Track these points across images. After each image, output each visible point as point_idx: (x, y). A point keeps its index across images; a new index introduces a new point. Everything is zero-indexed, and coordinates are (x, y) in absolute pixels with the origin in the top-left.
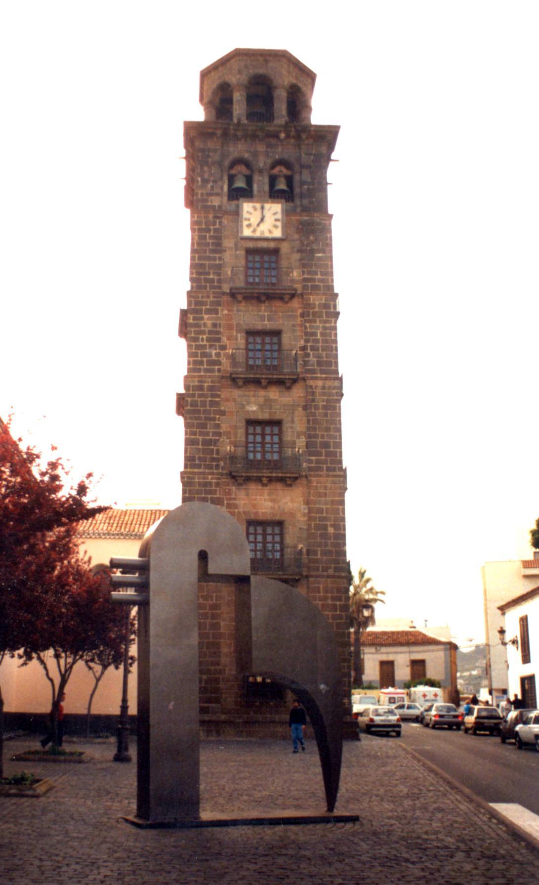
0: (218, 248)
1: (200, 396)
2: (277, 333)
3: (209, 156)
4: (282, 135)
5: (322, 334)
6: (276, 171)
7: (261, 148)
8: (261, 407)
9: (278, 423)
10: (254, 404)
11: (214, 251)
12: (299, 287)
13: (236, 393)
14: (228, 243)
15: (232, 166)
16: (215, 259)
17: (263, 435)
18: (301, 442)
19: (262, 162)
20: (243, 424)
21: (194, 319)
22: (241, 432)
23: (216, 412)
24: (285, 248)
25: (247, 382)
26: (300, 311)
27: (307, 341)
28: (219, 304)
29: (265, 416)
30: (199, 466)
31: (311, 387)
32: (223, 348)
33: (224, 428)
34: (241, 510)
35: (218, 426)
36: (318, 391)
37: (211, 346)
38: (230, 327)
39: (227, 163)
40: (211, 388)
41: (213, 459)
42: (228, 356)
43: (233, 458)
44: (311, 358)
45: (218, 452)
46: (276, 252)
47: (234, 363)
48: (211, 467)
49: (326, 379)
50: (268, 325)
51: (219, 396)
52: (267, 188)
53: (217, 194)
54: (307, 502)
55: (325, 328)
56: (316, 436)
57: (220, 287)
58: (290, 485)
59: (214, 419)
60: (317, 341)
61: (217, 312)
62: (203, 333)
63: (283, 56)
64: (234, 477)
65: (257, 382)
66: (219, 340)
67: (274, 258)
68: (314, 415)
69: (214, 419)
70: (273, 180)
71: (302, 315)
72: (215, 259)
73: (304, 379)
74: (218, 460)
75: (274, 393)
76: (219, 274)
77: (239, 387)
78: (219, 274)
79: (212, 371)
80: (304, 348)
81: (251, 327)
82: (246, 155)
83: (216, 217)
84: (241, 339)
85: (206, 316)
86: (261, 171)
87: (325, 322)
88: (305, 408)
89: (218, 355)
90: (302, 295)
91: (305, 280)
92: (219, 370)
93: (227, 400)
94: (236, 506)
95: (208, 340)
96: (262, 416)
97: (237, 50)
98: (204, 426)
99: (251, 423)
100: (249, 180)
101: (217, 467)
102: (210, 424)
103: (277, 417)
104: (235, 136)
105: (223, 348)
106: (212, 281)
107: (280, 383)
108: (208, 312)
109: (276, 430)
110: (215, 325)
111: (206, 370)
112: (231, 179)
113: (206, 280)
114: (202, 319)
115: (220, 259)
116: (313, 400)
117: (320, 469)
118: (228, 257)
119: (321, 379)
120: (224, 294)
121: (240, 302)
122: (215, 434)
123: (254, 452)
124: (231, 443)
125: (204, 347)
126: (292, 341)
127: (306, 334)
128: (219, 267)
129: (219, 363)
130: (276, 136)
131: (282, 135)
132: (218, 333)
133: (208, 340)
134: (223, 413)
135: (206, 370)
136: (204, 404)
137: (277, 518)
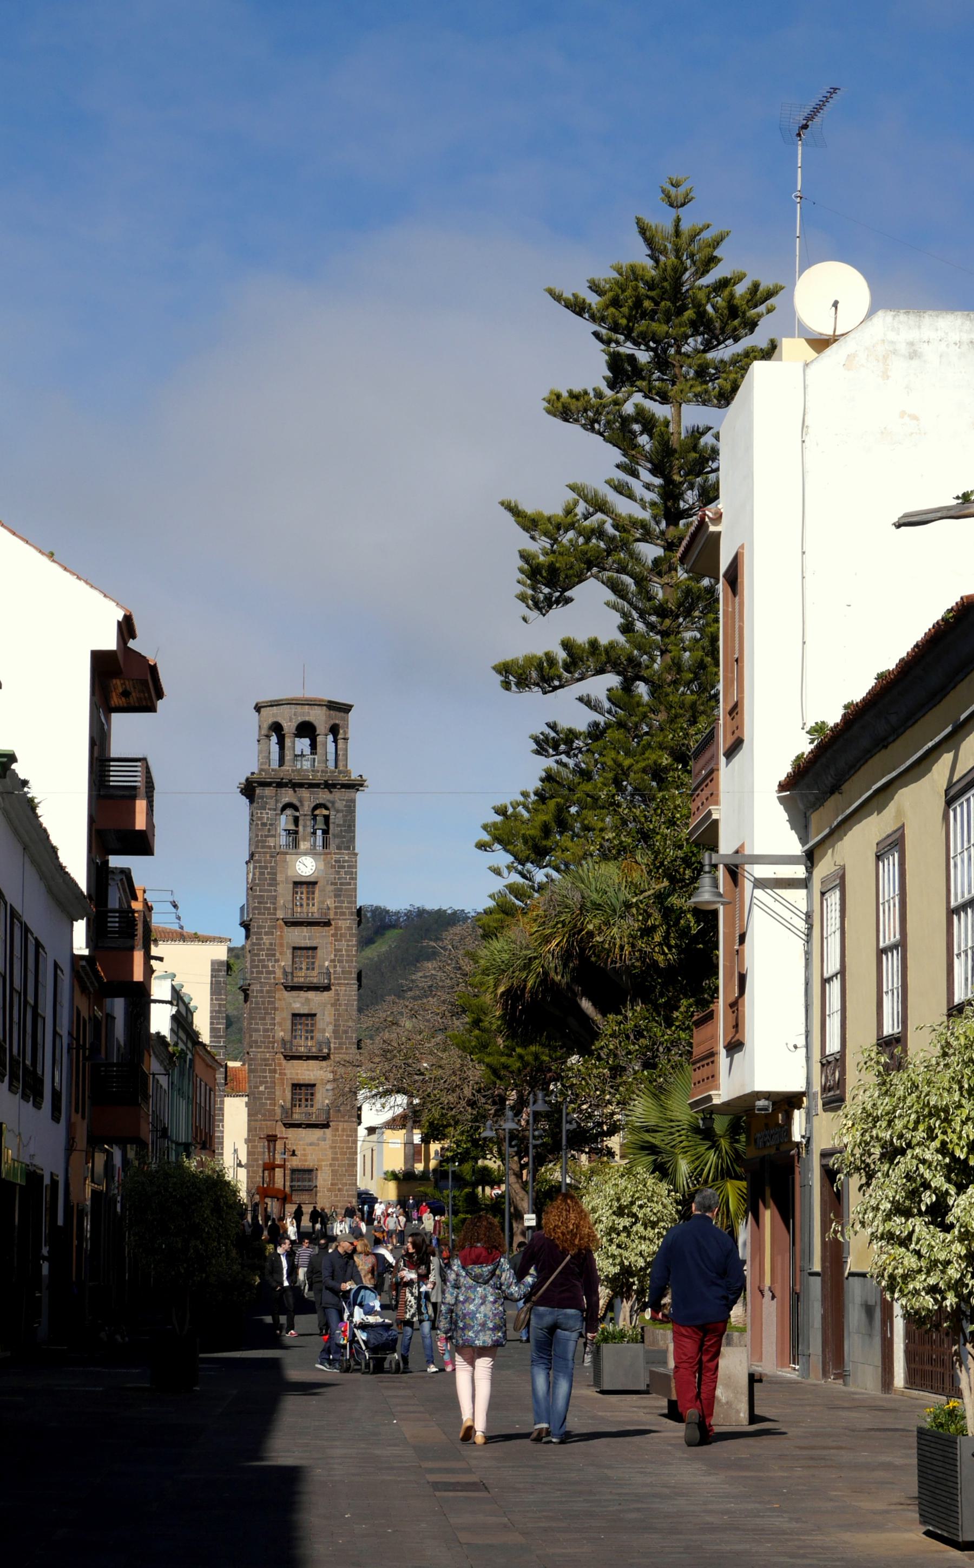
0: (274, 882)
1: (261, 997)
2: (315, 948)
3: (266, 803)
5: (346, 950)
6: (317, 812)
8: (303, 1004)
10: (298, 1002)
11: (270, 885)
13: (286, 994)
14: (280, 878)
16: (270, 891)
18: (331, 1028)
19: (306, 808)
20: (290, 1017)
21: (257, 939)
22: (289, 1023)
27: (335, 956)
28: (275, 927)
29: (306, 1012)
30: (260, 1047)
33: (277, 1020)
34: (289, 1076)
35: (274, 1019)
36: (342, 993)
37: (268, 960)
38: (281, 945)
39: (280, 805)
40: (268, 992)
41: (270, 1042)
44: (338, 969)
45: (274, 1037)
46: (315, 883)
48: (269, 1048)
50: (308, 943)
55: (348, 946)
56: (339, 1025)
57: (275, 914)
59: (271, 1014)
60: (342, 956)
61: (272, 934)
62: (263, 950)
66: (274, 955)
68: (338, 1010)
69: (271, 1014)
72: (270, 891)
75: (311, 995)
76: (274, 904)
78: (274, 904)
79: (269, 979)
80: (332, 961)
81: (297, 945)
87: (349, 941)
88: (332, 1005)
89: (273, 966)
93: (280, 1000)
94: (285, 1074)
95: (267, 955)
98: (264, 1019)
99: (295, 1015)
101: (273, 1048)
102: (268, 1017)
103: (313, 1012)
105: (277, 961)
106: (269, 909)
108: (266, 934)
110: (271, 944)
111: (265, 978)
113: (265, 908)
114: (262, 939)
115: (275, 891)
117: (342, 1048)
118: (280, 888)
127: (335, 950)
128: (275, 897)
129: (274, 972)
132: (275, 950)
133: (267, 955)
135: (265, 978)
136: (263, 1003)
137: (312, 1082)
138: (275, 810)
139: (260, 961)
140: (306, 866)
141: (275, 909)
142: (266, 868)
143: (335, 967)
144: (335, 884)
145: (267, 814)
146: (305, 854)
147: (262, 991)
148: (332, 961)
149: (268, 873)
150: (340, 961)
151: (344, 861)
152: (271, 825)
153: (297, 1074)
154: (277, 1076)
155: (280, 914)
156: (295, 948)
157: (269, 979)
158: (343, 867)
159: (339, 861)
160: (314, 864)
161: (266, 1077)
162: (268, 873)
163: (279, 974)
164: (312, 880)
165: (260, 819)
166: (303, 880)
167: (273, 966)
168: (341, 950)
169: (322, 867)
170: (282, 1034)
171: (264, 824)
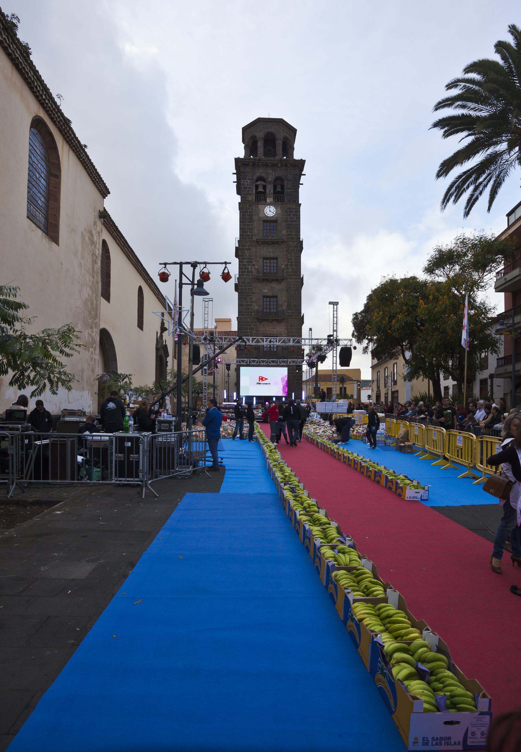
0: (251, 220)
2: (276, 259)
4: (279, 165)
7: (270, 171)
9: (276, 297)
11: (249, 222)
12: (285, 238)
14: (255, 218)
15: (257, 181)
17: (270, 301)
19: (270, 178)
23: (251, 293)
24: (280, 221)
25: (263, 280)
26: (286, 249)
27: (288, 262)
29: (271, 294)
30: (244, 315)
31: (289, 282)
32: (254, 265)
35: (251, 299)
37: (248, 265)
42: (255, 268)
43: (257, 312)
44: (290, 270)
45: (252, 309)
47: (258, 272)
49: (296, 278)
50: (272, 255)
51: (252, 286)
52: (272, 191)
53: (251, 194)
54: (287, 329)
57: (252, 238)
58: (280, 322)
59: (250, 296)
60: (292, 262)
62: (245, 259)
63: (281, 122)
64: (258, 319)
65: (267, 280)
66: (252, 262)
67: (275, 224)
69: (250, 296)
70: (275, 187)
71: (286, 251)
73: (287, 279)
74: (251, 312)
75: (274, 285)
76: (252, 233)
77: (260, 282)
78: (252, 233)
80: (287, 265)
82: (263, 175)
83: (250, 206)
84: (261, 261)
85: (246, 252)
86: (270, 183)
88: (287, 291)
89: (251, 268)
90: (286, 242)
91: (288, 235)
92: (252, 275)
94: (259, 331)
96: (269, 294)
97: (259, 118)
99: (264, 297)
100: (265, 187)
103: (275, 295)
104: (259, 165)
105: (254, 265)
106: (249, 235)
107: (277, 280)
108: (247, 250)
109: (275, 299)
110: (250, 255)
111: (247, 275)
112: (257, 187)
114: (245, 253)
115: (252, 225)
116: (290, 288)
119: (294, 278)
120: (254, 241)
121: (260, 245)
122: (250, 302)
123: (266, 309)
124: (257, 305)
125: (246, 265)
126: (283, 298)
129: (252, 272)
130: (277, 166)
131: (279, 165)
132: (251, 259)
134: (253, 293)
135: (247, 275)
138: (251, 180)
139: (243, 265)
140: (270, 211)
141: (252, 235)
142: (247, 212)
143: (288, 268)
144: (288, 221)
145: (247, 182)
146: (270, 204)
147: (245, 283)
148: (287, 265)
149: (248, 215)
150: (291, 265)
151: (293, 209)
152: (249, 188)
153: (266, 331)
154: (254, 332)
155: (255, 239)
156: (264, 258)
157: (249, 275)
158: (292, 212)
159: (290, 209)
160: (275, 210)
161: (247, 332)
162: (248, 215)
163: (255, 273)
164: (274, 219)
165: (244, 185)
166: (269, 219)
167: (251, 268)
168: (291, 259)
169: (279, 211)
170: (257, 307)
171: (245, 188)
